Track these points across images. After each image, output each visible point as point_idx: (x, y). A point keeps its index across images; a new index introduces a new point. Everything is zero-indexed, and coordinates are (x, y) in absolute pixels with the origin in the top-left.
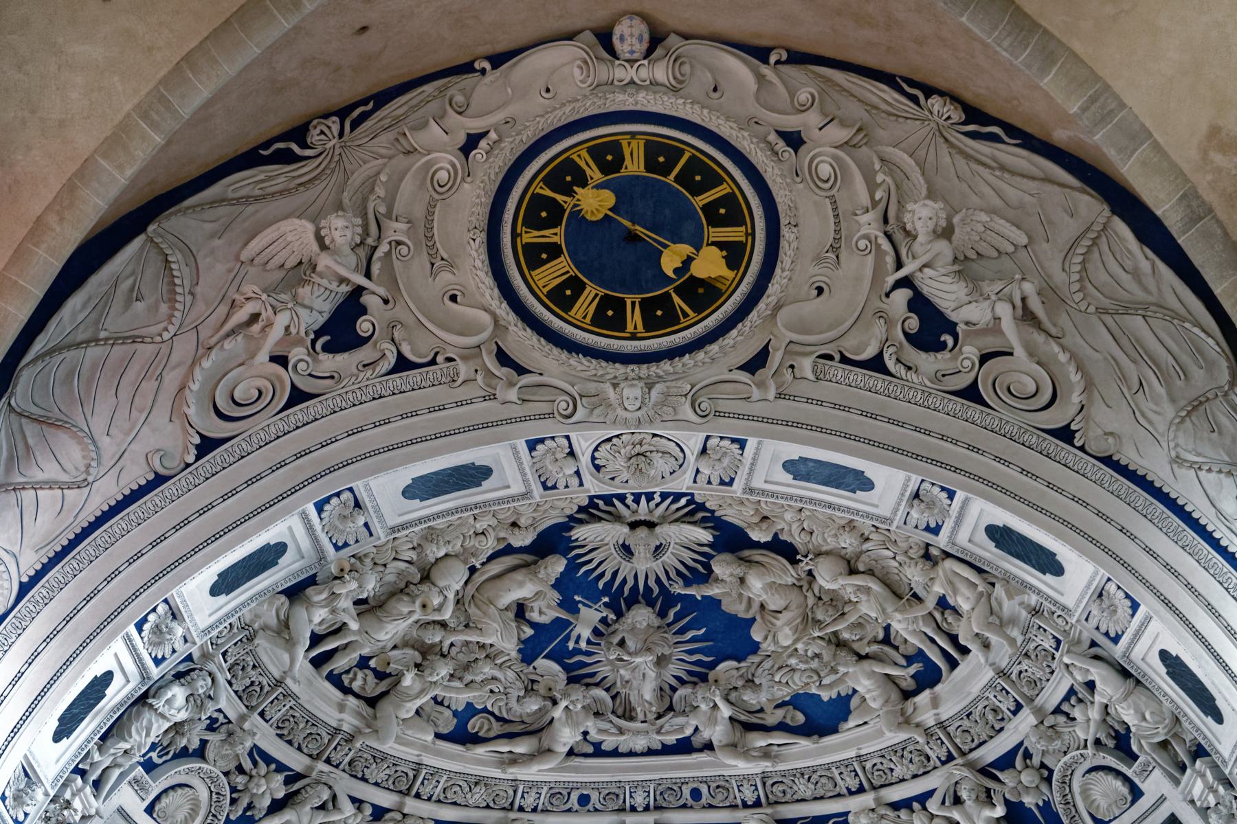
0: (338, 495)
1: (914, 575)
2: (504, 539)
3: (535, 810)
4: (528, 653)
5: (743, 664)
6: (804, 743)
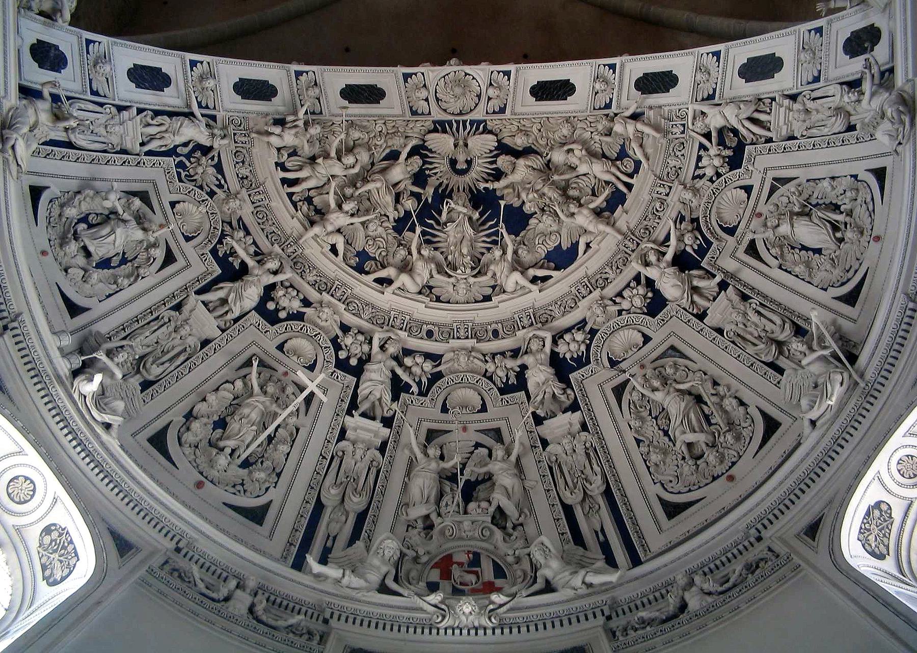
0: (307, 72)
3: (401, 329)
4: (402, 225)
5: (518, 238)
6: (554, 273)
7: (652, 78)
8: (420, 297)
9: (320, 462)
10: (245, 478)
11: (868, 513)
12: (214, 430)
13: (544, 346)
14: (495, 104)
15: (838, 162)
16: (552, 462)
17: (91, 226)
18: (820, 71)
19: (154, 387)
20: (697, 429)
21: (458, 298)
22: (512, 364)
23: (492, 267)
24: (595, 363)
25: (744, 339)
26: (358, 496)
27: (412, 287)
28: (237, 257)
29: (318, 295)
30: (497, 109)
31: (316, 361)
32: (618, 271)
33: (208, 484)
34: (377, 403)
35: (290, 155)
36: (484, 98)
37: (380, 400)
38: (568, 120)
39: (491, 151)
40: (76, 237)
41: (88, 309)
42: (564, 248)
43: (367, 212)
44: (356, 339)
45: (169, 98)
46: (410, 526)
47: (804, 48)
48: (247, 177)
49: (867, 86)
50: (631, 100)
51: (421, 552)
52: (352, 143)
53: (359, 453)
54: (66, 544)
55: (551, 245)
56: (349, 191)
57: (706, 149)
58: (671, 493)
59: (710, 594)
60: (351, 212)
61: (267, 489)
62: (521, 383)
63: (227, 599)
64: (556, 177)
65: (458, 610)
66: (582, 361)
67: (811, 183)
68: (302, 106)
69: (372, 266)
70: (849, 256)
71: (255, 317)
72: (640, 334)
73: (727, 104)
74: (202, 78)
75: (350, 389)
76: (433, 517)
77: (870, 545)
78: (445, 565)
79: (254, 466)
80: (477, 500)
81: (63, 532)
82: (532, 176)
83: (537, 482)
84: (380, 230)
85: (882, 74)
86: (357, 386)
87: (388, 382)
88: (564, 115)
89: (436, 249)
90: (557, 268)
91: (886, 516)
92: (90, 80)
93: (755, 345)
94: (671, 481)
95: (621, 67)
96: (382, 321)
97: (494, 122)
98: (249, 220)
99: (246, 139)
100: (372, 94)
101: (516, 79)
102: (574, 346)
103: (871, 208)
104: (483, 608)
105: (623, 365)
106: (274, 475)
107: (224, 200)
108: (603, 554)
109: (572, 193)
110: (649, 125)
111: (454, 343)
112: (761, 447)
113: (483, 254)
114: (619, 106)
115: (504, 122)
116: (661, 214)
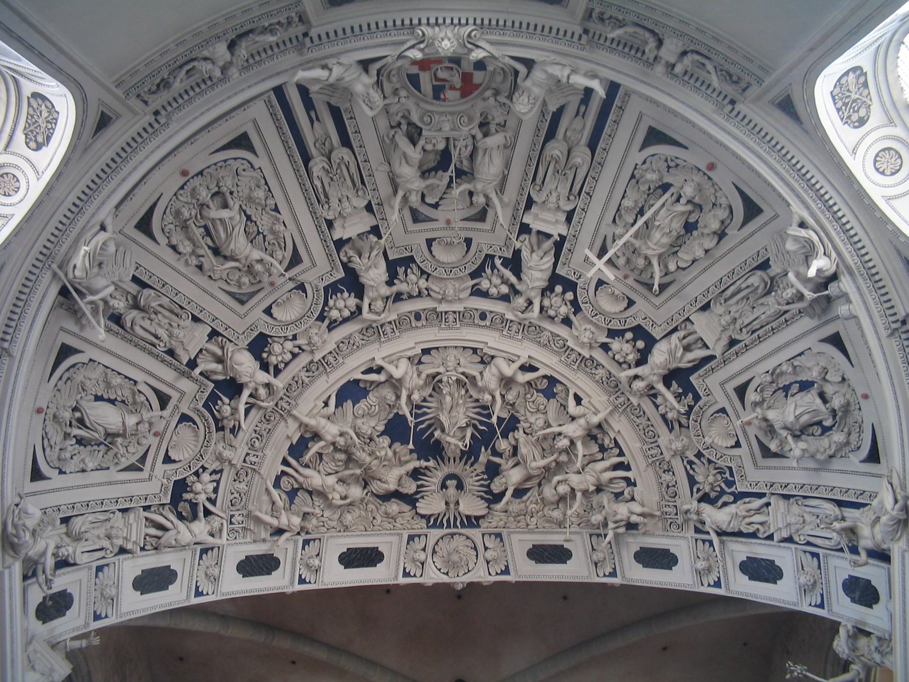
0: (605, 575)
2: (522, 502)
3: (511, 321)
4: (511, 425)
5: (395, 411)
6: (360, 376)
7: (262, 569)
8: (492, 353)
9: (592, 189)
10: (666, 173)
11: (49, 138)
12: (697, 221)
13: (370, 305)
14: (418, 544)
15: (78, 487)
16: (362, 189)
17: (819, 423)
18: (96, 576)
19: (756, 264)
20: (218, 222)
21: (455, 352)
22: (401, 287)
23: (421, 382)
24: (319, 288)
25: (172, 312)
26: (554, 156)
27: (500, 362)
28: (674, 393)
29: (593, 355)
30: (416, 539)
31: (596, 289)
32: (296, 379)
33: (703, 168)
34: (535, 248)
35: (622, 493)
36: (429, 550)
37: (532, 251)
38: (346, 528)
39: (422, 497)
40: (834, 413)
41: (823, 341)
42: (350, 402)
43: (545, 437)
44: (556, 311)
45: (741, 550)
46: (503, 126)
47: (113, 600)
48: (664, 472)
49: (50, 562)
50: (284, 549)
51: (492, 100)
52: (560, 506)
53: (553, 199)
54: (844, 108)
55: (362, 405)
56: (564, 458)
57: (209, 499)
58: (243, 159)
59: (206, 59)
60: (561, 437)
61: (644, 162)
62: (393, 268)
63: (684, 53)
64: (358, 471)
65: (455, 43)
66: (332, 290)
67: (105, 465)
68: (610, 543)
69: (541, 384)
70: (67, 394)
71: (656, 333)
72: (274, 316)
73: (188, 545)
74: (709, 570)
75: (562, 262)
76: (479, 135)
77: (47, 107)
78: (468, 88)
79: (657, 185)
80: (436, 152)
81: (846, 120)
82: (382, 473)
83: (377, 170)
84: (532, 420)
85: (34, 574)
86: (555, 265)
87: (524, 269)
88: (350, 534)
89: (477, 401)
90: (357, 381)
91: (31, 136)
92: (819, 567)
93: (161, 305)
94: (244, 170)
95: (294, 580)
96: (530, 329)
97: (420, 526)
98: (662, 429)
99: (666, 509)
100: (540, 554)
101: (397, 570)
102: (341, 304)
103: (46, 441)
104: (431, 45)
105: (291, 285)
106: (637, 176)
107: (687, 449)
108: (311, 98)
109: (342, 456)
110: (265, 524)
111: (459, 307)
112: (155, 204)
113: (431, 396)
114: (296, 542)
115: (409, 527)
116: (254, 435)
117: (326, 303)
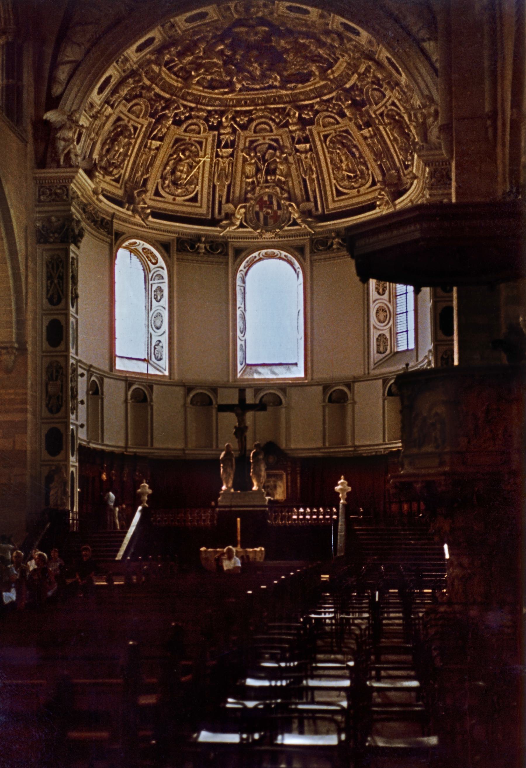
1: (323, 38)
4: (225, 63)
33: (177, 198)
45: (113, 81)
46: (248, 184)
66: (311, 122)
71: (172, 127)
117: (315, 116)
